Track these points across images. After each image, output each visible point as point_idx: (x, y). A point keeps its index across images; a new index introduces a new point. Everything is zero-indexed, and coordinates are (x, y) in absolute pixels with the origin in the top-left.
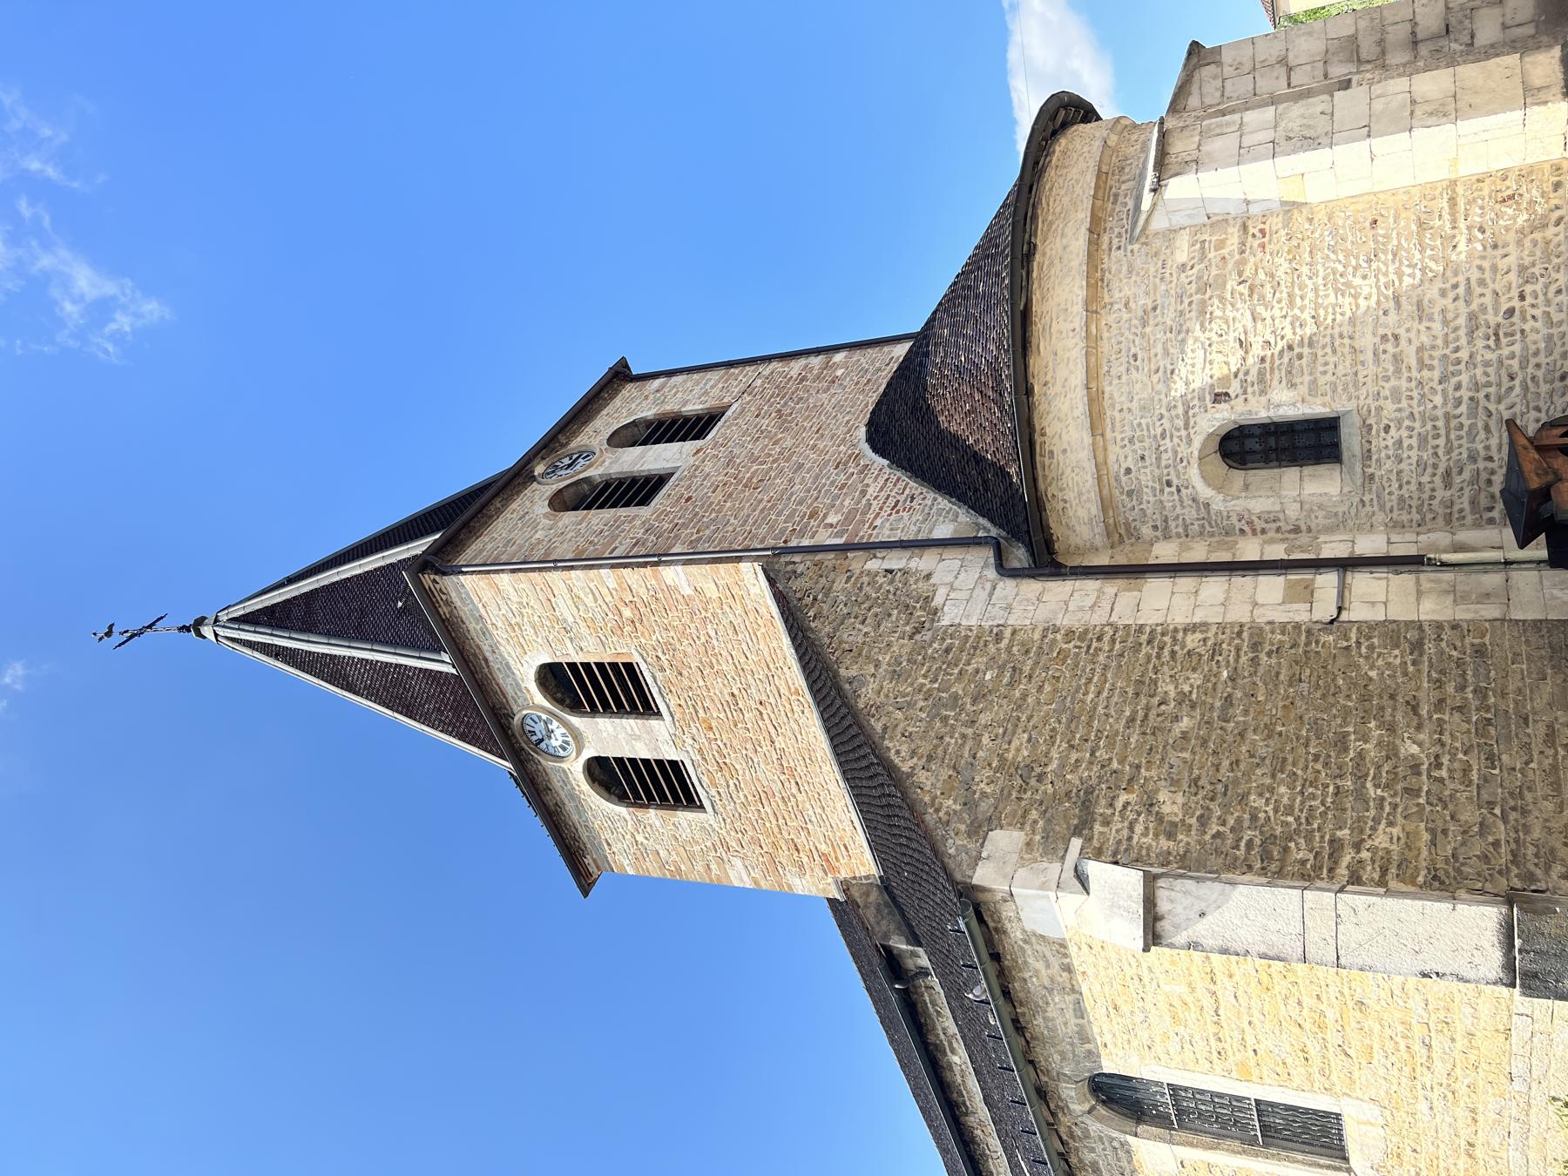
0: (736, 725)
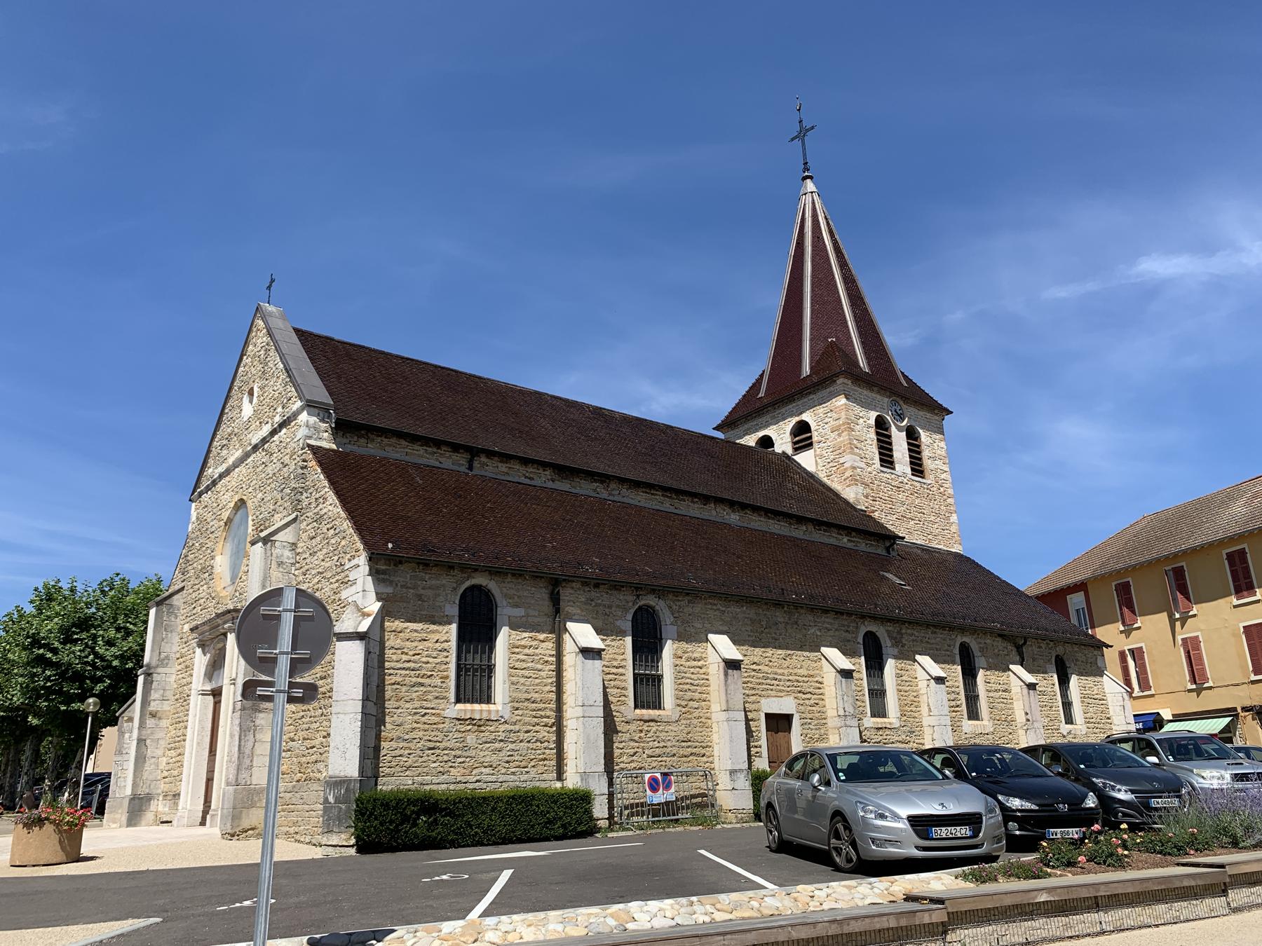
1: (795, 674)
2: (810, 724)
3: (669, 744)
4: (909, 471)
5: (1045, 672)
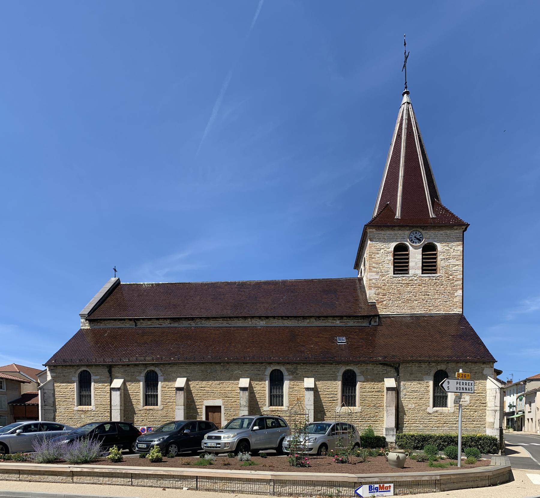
1: (224, 390)
2: (230, 409)
3: (158, 417)
4: (420, 271)
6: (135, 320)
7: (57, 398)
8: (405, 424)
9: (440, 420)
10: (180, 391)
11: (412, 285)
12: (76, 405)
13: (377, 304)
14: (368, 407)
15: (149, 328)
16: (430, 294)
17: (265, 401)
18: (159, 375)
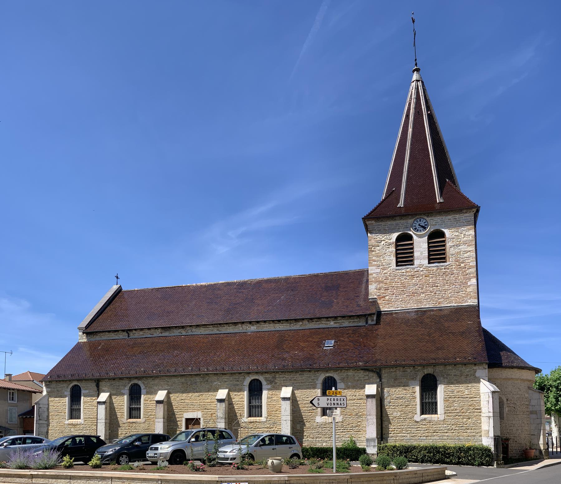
0: (428, 284)
1: (204, 402)
3: (140, 430)
4: (427, 261)
5: (407, 386)
6: (128, 331)
7: (51, 412)
8: (391, 433)
9: (429, 429)
10: (160, 404)
11: (418, 277)
12: (67, 419)
13: (378, 299)
14: (350, 416)
15: (141, 338)
16: (439, 285)
17: (243, 412)
18: (142, 388)
